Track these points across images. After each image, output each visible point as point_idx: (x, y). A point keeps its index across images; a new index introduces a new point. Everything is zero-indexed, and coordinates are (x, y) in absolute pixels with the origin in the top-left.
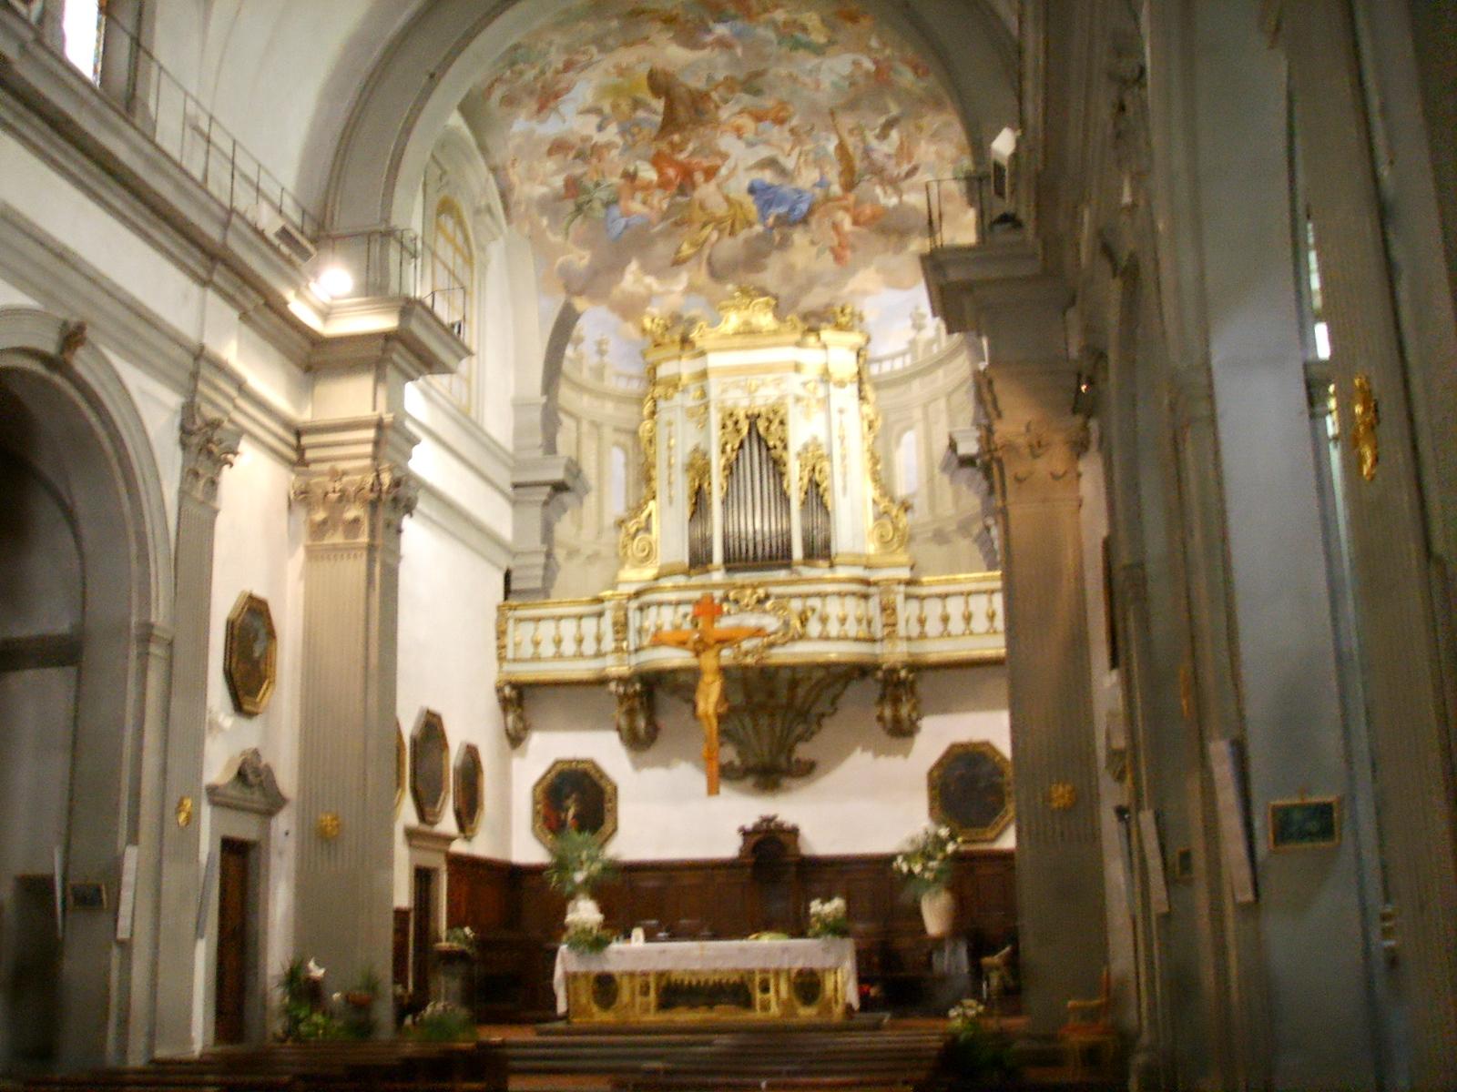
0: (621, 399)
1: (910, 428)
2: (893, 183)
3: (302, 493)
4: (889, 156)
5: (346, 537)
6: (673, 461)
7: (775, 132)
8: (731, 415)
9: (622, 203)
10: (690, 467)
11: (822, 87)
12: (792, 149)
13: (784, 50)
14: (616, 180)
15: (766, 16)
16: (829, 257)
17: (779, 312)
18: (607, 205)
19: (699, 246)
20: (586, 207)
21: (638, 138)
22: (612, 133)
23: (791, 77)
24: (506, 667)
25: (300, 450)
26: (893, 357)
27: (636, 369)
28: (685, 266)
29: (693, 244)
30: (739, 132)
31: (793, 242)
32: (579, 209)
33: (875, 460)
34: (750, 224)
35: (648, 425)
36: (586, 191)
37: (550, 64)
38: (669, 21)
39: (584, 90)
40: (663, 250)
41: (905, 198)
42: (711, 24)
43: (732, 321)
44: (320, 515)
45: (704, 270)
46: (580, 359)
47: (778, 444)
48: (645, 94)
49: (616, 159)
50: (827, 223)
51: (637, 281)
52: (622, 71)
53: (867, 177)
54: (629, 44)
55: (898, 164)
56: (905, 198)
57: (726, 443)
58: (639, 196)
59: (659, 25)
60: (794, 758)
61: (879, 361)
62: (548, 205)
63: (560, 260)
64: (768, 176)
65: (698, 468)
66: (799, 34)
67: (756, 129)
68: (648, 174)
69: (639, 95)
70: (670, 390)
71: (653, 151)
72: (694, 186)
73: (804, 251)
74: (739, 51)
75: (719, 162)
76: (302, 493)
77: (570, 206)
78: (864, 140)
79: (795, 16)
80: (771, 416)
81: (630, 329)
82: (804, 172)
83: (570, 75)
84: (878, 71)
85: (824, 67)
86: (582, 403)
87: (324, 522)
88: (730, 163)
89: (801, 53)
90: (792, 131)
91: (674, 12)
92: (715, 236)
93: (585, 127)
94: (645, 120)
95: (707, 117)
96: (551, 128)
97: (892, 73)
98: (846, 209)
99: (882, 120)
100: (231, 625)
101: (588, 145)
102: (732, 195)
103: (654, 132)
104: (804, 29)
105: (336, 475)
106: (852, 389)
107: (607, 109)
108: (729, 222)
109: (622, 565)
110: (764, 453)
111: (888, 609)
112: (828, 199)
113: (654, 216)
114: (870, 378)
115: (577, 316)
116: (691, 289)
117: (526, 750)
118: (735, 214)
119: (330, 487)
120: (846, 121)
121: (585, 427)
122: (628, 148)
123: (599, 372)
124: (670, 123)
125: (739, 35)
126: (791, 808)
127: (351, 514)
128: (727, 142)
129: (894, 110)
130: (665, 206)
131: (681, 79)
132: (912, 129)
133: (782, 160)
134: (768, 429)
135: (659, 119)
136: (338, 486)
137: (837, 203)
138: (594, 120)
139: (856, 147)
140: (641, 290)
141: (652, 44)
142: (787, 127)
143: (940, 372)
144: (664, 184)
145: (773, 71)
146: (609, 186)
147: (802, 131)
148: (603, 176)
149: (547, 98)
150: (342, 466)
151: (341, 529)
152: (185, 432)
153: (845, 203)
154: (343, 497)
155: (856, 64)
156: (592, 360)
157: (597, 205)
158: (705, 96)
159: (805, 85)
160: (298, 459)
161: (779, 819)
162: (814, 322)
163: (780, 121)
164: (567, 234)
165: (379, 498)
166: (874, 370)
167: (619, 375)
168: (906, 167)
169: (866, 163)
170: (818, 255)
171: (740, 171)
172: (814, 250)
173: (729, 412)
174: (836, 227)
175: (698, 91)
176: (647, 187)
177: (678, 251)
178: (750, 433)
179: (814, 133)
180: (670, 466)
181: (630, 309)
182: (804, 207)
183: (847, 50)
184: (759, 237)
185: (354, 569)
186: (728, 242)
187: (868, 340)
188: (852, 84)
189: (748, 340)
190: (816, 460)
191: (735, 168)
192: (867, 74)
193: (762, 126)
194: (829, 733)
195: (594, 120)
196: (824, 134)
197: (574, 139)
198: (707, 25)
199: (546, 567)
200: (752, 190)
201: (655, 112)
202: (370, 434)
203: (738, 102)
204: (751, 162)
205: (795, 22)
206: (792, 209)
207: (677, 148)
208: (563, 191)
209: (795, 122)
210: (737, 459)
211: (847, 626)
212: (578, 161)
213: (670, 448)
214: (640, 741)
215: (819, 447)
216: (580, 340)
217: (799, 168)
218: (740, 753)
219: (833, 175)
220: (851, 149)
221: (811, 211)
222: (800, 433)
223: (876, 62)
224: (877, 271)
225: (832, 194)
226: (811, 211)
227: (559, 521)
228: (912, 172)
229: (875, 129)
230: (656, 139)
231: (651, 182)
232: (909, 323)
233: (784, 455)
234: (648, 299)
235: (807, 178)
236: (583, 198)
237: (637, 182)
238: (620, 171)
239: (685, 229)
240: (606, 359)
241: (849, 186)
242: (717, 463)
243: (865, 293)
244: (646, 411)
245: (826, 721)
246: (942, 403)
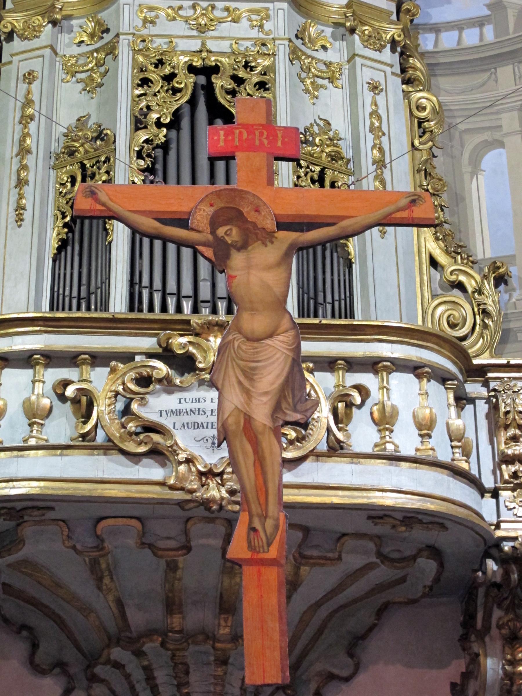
1: (502, 145)
8: (160, 63)
70: (38, 20)
80: (241, 74)
134: (233, 93)
178: (192, 102)
210: (165, 147)
211: (432, 443)
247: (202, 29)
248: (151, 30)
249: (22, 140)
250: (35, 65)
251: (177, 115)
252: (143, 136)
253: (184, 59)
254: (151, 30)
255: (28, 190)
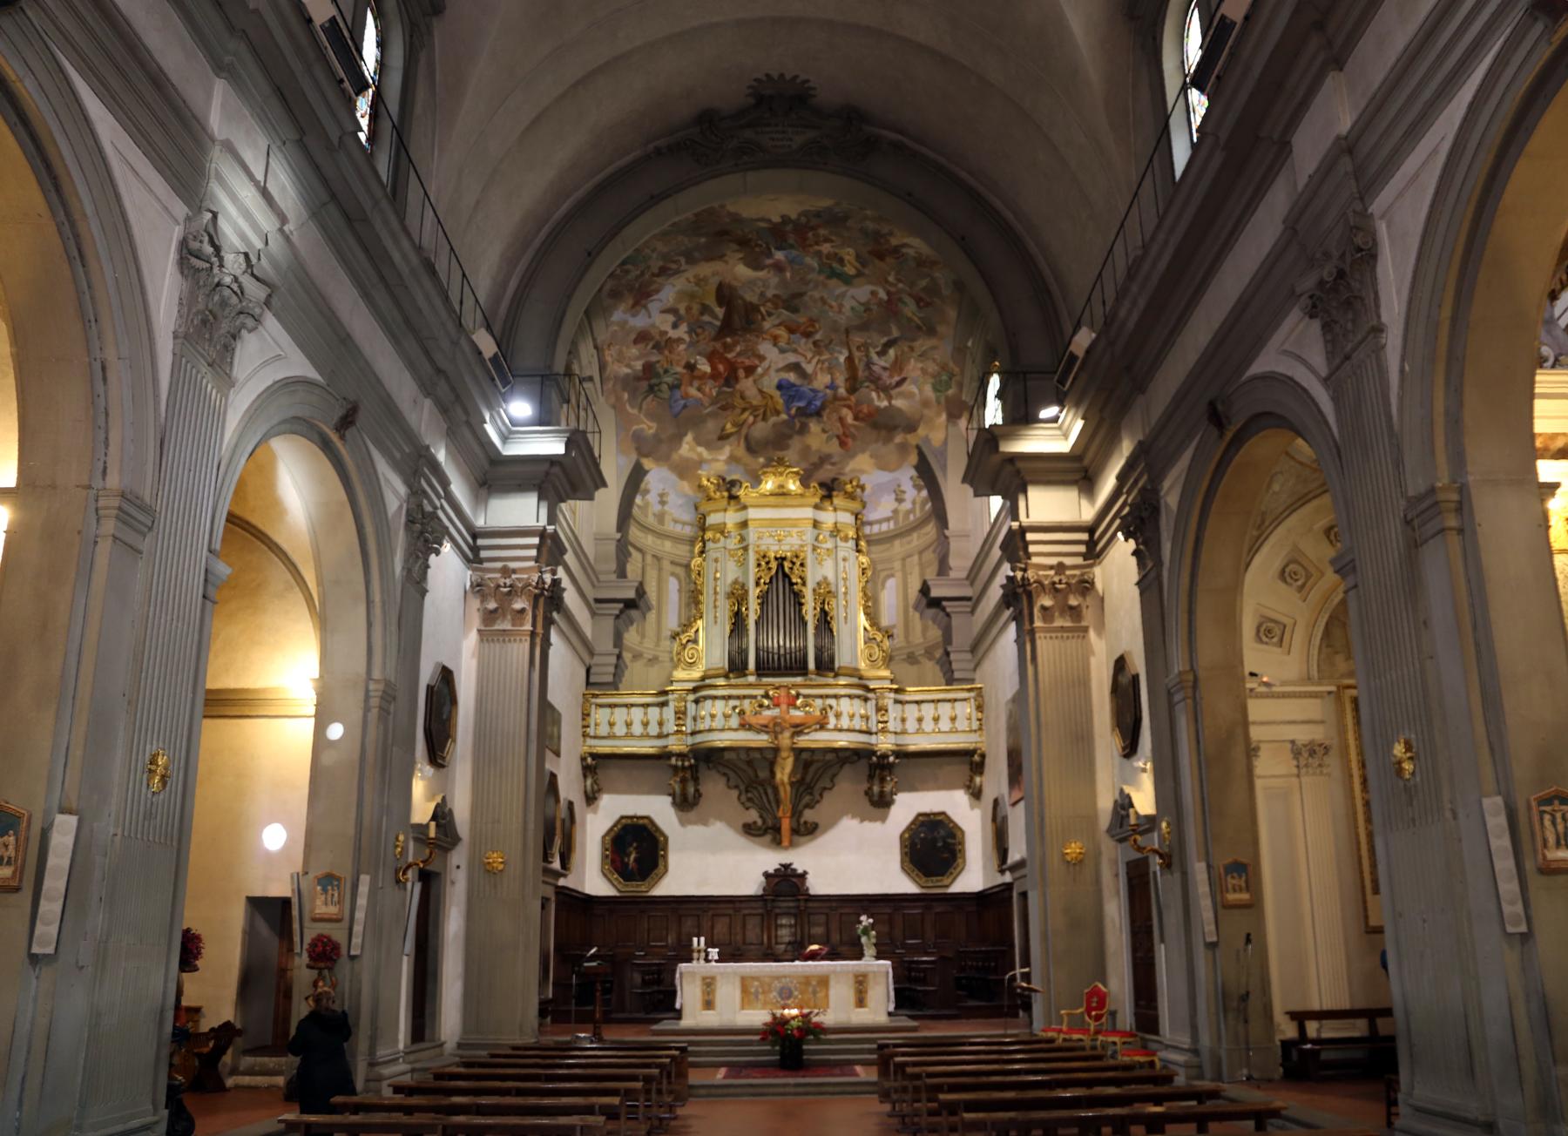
0: (676, 539)
2: (885, 390)
3: (478, 585)
4: (885, 369)
5: (513, 625)
6: (718, 589)
7: (804, 345)
8: (764, 557)
9: (683, 388)
10: (731, 595)
11: (843, 310)
12: (812, 358)
13: (822, 278)
14: (679, 369)
15: (816, 248)
16: (835, 441)
17: (805, 482)
18: (673, 387)
19: (739, 425)
20: (656, 388)
21: (701, 337)
22: (682, 332)
23: (822, 299)
24: (590, 742)
25: (475, 549)
26: (880, 522)
27: (688, 516)
28: (727, 441)
29: (734, 425)
30: (775, 340)
31: (809, 432)
32: (651, 389)
33: (866, 596)
34: (778, 413)
35: (697, 561)
36: (658, 375)
37: (649, 267)
38: (743, 243)
39: (669, 293)
40: (711, 426)
41: (893, 402)
42: (773, 250)
43: (769, 485)
44: (492, 605)
45: (742, 440)
46: (647, 505)
47: (799, 581)
48: (711, 301)
49: (683, 353)
50: (835, 416)
51: (692, 449)
52: (700, 281)
53: (866, 384)
54: (709, 259)
55: (891, 376)
56: (893, 402)
57: (759, 579)
58: (696, 383)
59: (735, 247)
60: (802, 820)
61: (870, 524)
62: (629, 383)
63: (635, 427)
64: (792, 377)
65: (738, 596)
66: (835, 265)
67: (789, 339)
68: (705, 367)
69: (707, 302)
70: (718, 535)
71: (709, 349)
72: (737, 379)
73: (817, 437)
74: (788, 275)
75: (757, 362)
76: (478, 585)
77: (644, 385)
78: (867, 356)
79: (837, 251)
80: (795, 560)
81: (686, 486)
82: (819, 376)
83: (659, 280)
84: (889, 301)
85: (849, 294)
86: (648, 541)
87: (495, 610)
88: (766, 364)
89: (833, 282)
90: (815, 343)
91: (750, 236)
92: (751, 419)
93: (664, 323)
94: (710, 323)
95: (752, 326)
96: (639, 322)
97: (900, 304)
98: (849, 407)
99: (884, 340)
100: (430, 689)
101: (665, 338)
102: (765, 390)
103: (713, 333)
104: (841, 261)
105: (506, 572)
106: (851, 544)
107: (682, 311)
108: (762, 411)
109: (675, 667)
110: (787, 585)
111: (881, 709)
112: (836, 398)
113: (706, 401)
114: (865, 536)
115: (646, 472)
116: (732, 459)
117: (598, 806)
118: (766, 405)
119: (501, 582)
120: (857, 339)
121: (649, 559)
122: (692, 344)
123: (661, 517)
124: (727, 328)
125: (791, 262)
126: (802, 858)
127: (518, 605)
128: (765, 348)
129: (895, 333)
130: (714, 394)
131: (741, 292)
132: (906, 349)
133: (804, 365)
134: (791, 569)
135: (718, 323)
136: (508, 582)
137: (842, 403)
138: (671, 318)
139: (860, 360)
140: (695, 457)
141: (726, 262)
142: (811, 340)
143: (915, 535)
144: (715, 376)
145: (809, 293)
146: (675, 374)
147: (822, 344)
148: (672, 365)
149: (641, 295)
150: (513, 565)
151: (509, 617)
152: (410, 521)
153: (848, 402)
154: (513, 592)
155: (873, 293)
156: (657, 508)
157: (665, 387)
158: (752, 309)
159: (831, 307)
160: (473, 557)
161: (793, 867)
162: (829, 490)
163: (807, 335)
164: (640, 409)
165: (542, 594)
166: (867, 530)
167: (676, 521)
168: (897, 378)
169: (866, 373)
170: (829, 439)
171: (772, 372)
172: (825, 436)
173: (762, 554)
174: (841, 420)
175: (751, 303)
176: (703, 376)
177: (723, 429)
179: (832, 346)
180: (716, 593)
181: (685, 470)
182: (818, 403)
183: (870, 283)
184: (784, 422)
185: (519, 650)
186: (760, 425)
187: (864, 507)
188: (867, 310)
189: (780, 500)
190: (825, 594)
191: (770, 367)
192: (880, 303)
193: (792, 336)
194: (829, 802)
195: (671, 318)
196: (838, 348)
197: (653, 332)
198: (771, 252)
199: (616, 667)
200: (780, 387)
201: (716, 317)
202: (536, 541)
203: (778, 317)
204: (781, 365)
205: (836, 254)
206: (809, 403)
207: (728, 348)
208: (641, 374)
209: (818, 337)
212: (655, 351)
213: (716, 579)
214: (685, 804)
215: (828, 584)
216: (647, 491)
217: (816, 374)
218: (761, 817)
219: (841, 380)
220: (857, 361)
221: (823, 407)
222: (817, 572)
223: (888, 293)
224: (871, 456)
225: (839, 395)
226: (823, 407)
227: (628, 630)
228: (899, 384)
229: (877, 346)
230: (716, 339)
231: (706, 373)
232: (893, 496)
233: (804, 589)
234: (700, 463)
235: (822, 381)
236: (654, 381)
237: (696, 373)
238: (683, 363)
239: (729, 412)
240: (666, 508)
241: (852, 389)
242: (754, 593)
243: (862, 472)
244: (698, 546)
245: (826, 794)
246: (916, 558)
247: (779, 541)
248: (760, 542)
249: (715, 589)
250: (718, 555)
251: (771, 579)
252: (758, 590)
253: (773, 555)
254: (760, 542)
255: (718, 610)
